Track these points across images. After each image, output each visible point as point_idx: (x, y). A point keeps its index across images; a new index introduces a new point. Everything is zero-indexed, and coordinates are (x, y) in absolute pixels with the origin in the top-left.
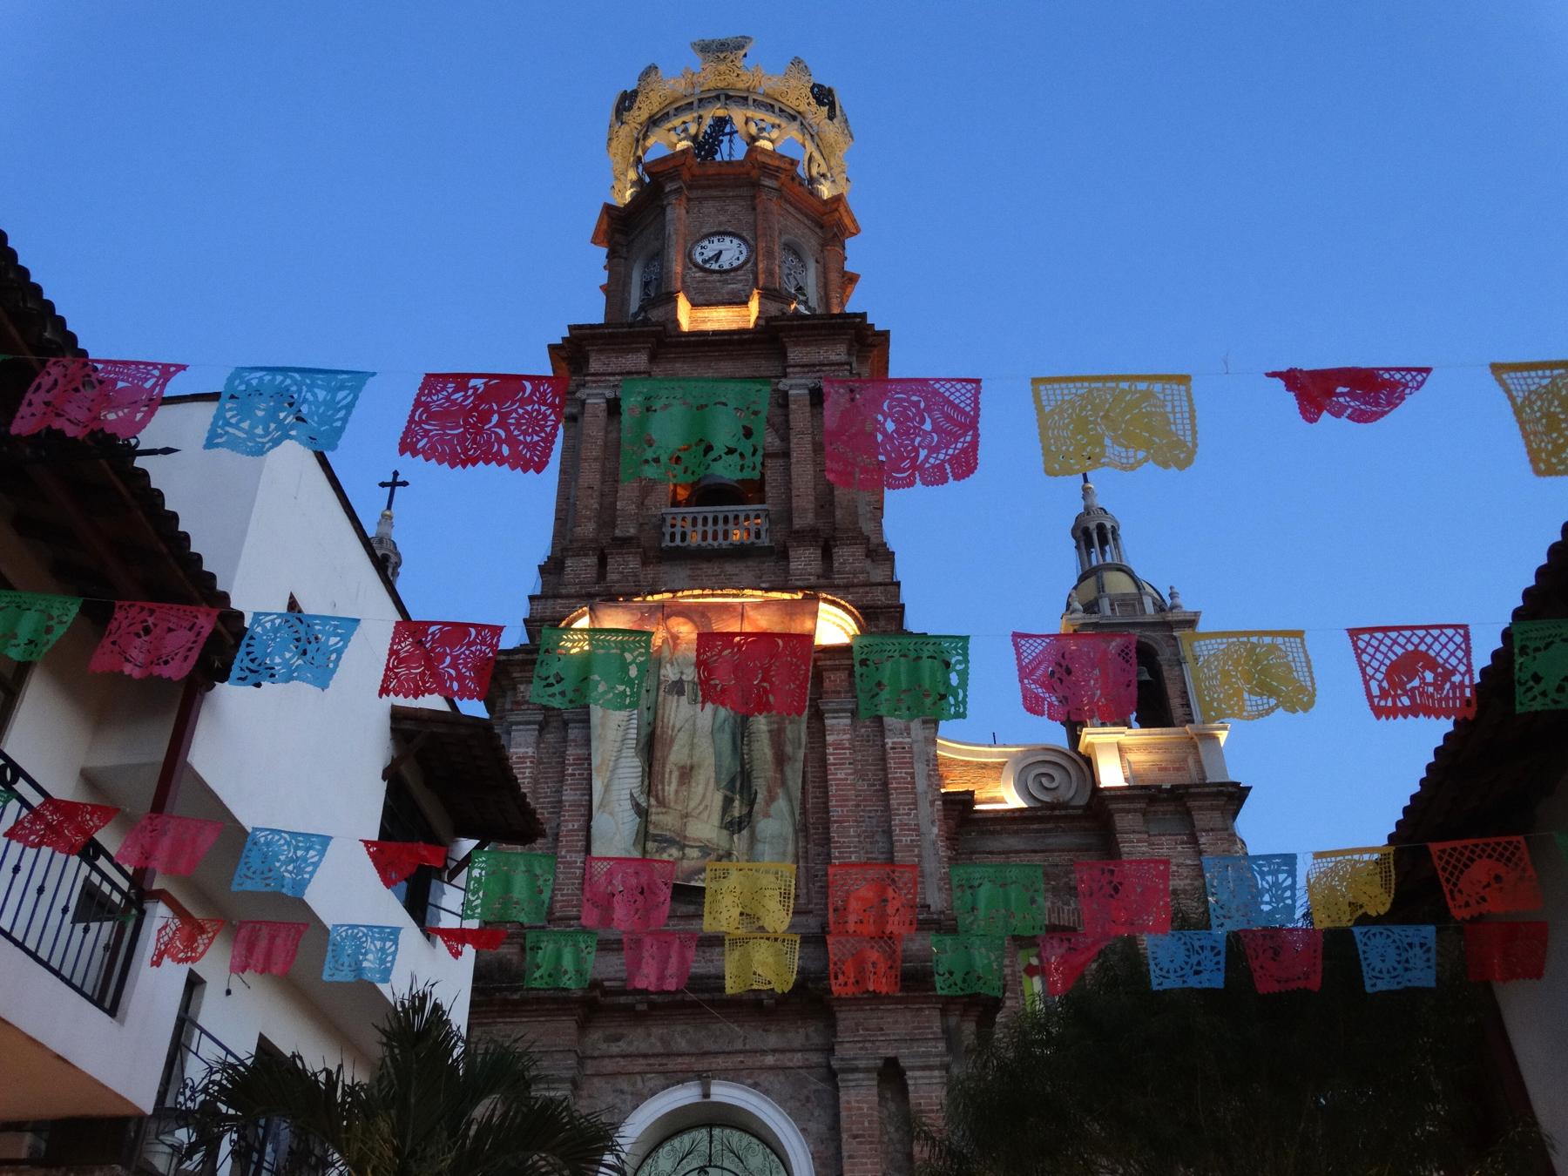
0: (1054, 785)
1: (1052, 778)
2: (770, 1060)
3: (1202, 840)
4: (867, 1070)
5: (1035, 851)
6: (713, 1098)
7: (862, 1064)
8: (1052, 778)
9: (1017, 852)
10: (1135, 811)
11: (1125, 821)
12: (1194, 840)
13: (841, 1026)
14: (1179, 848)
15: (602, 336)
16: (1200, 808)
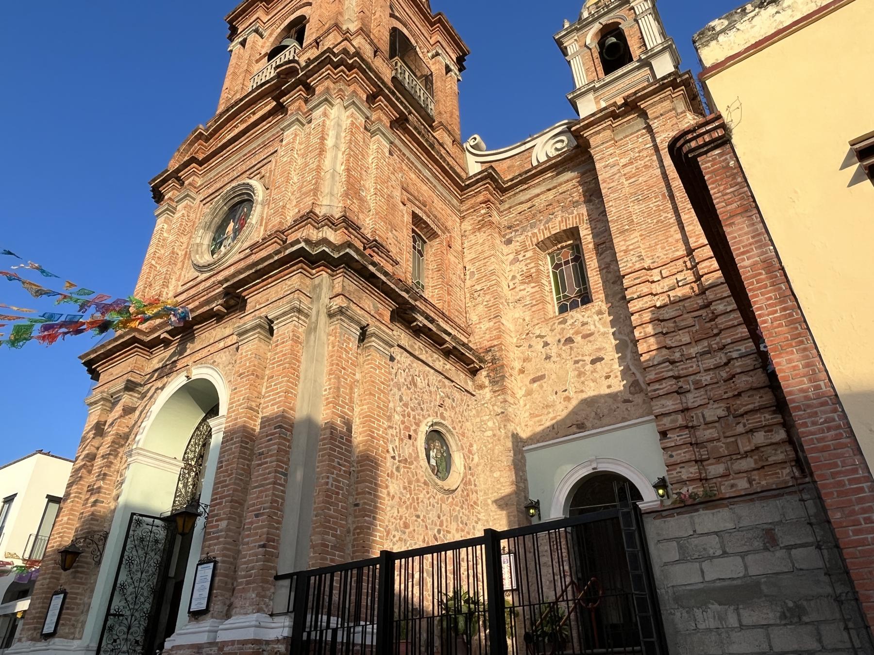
0: (565, 144)
1: (562, 141)
2: (222, 345)
3: (654, 126)
4: (253, 329)
5: (549, 190)
6: (193, 378)
7: (248, 326)
8: (562, 141)
9: (538, 195)
10: (604, 129)
11: (599, 142)
12: (649, 129)
13: (248, 308)
14: (640, 140)
15: (239, 15)
16: (652, 105)
